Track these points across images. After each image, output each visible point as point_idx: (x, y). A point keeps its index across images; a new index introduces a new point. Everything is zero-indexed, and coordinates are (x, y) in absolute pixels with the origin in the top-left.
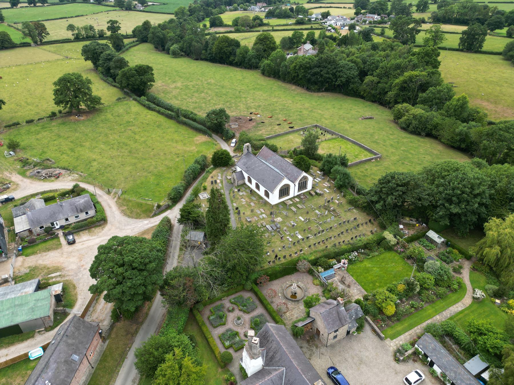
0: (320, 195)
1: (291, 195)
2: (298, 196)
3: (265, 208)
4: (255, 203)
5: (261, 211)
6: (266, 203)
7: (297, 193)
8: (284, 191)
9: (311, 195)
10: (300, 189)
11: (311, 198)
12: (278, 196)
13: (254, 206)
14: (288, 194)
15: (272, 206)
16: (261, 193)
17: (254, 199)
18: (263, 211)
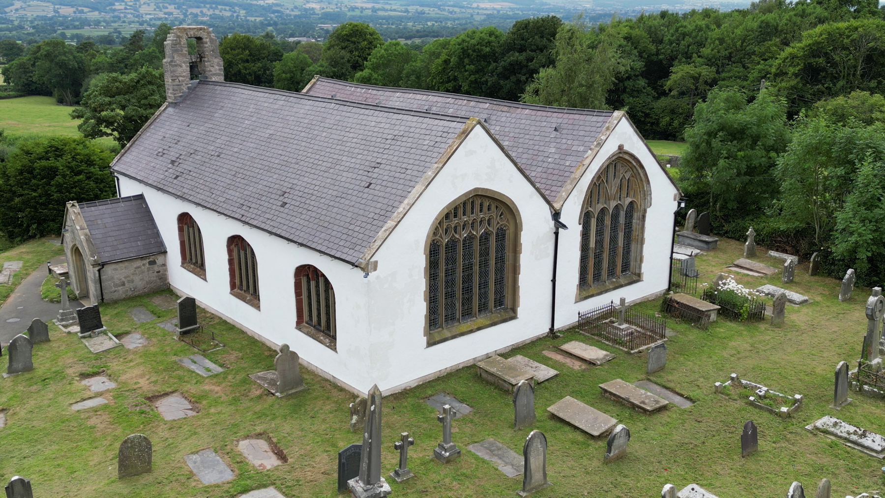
0: (756, 316)
1: (530, 321)
2: (587, 328)
3: (286, 428)
4: (195, 402)
5: (239, 463)
6: (300, 386)
7: (567, 317)
8: (470, 267)
9: (693, 317)
10: (592, 277)
11: (693, 335)
12: (421, 308)
13: (174, 426)
14: (502, 303)
15: (367, 410)
16: (273, 319)
17: (202, 366)
18: (271, 462)
